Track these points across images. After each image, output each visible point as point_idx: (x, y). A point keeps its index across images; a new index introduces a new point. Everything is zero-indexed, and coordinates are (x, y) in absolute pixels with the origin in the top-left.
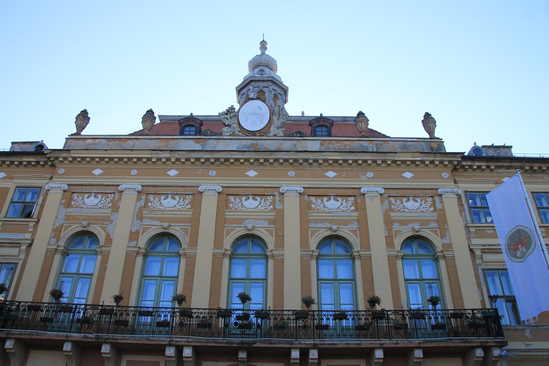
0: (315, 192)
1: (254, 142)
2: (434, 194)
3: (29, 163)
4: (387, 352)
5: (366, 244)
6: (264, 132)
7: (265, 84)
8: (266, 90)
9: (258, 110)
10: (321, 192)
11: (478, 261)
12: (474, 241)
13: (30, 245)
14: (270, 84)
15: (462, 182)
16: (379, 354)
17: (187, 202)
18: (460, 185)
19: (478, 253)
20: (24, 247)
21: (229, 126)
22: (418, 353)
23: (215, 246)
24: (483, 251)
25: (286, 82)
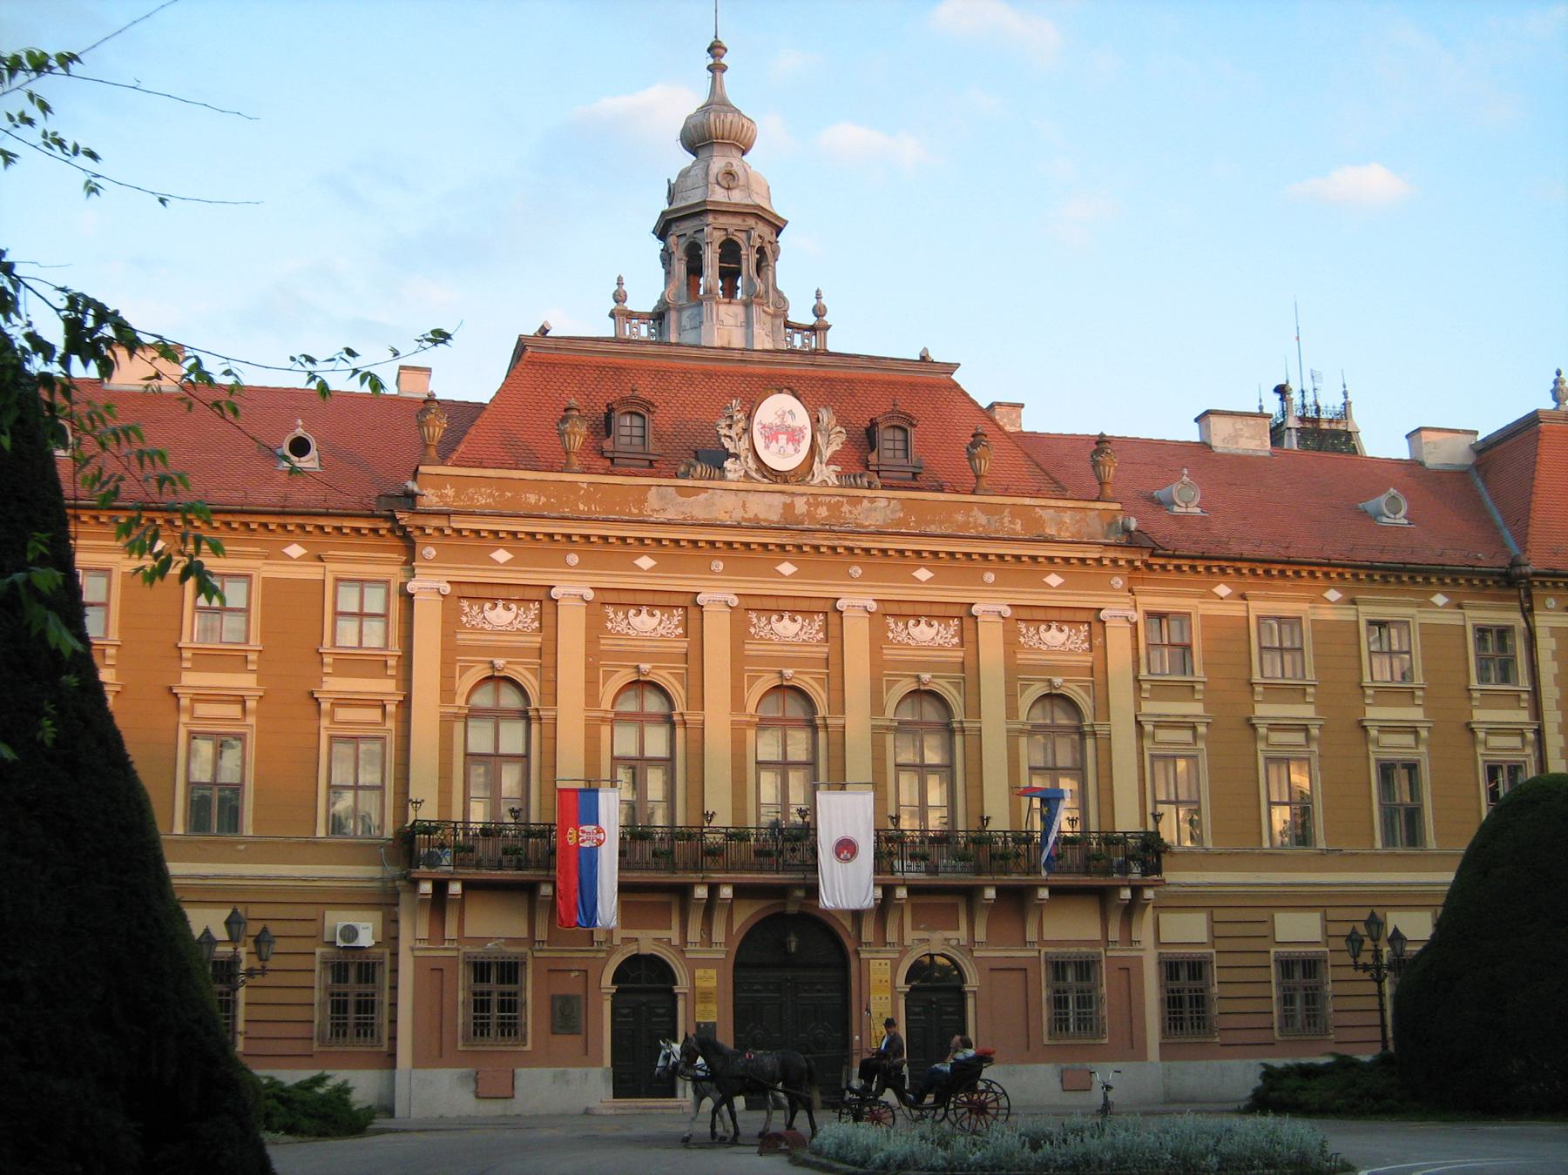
0: (894, 609)
1: (788, 500)
2: (1094, 621)
3: (357, 530)
4: (1000, 890)
5: (974, 709)
6: (803, 473)
7: (737, 221)
8: (740, 238)
9: (789, 421)
10: (907, 609)
11: (1147, 743)
12: (1147, 707)
13: (406, 704)
14: (751, 222)
15: (1143, 593)
16: (990, 893)
17: (675, 621)
18: (1139, 599)
19: (1148, 728)
20: (391, 708)
21: (737, 456)
22: (1044, 893)
23: (733, 708)
24: (1157, 725)
25: (779, 208)
